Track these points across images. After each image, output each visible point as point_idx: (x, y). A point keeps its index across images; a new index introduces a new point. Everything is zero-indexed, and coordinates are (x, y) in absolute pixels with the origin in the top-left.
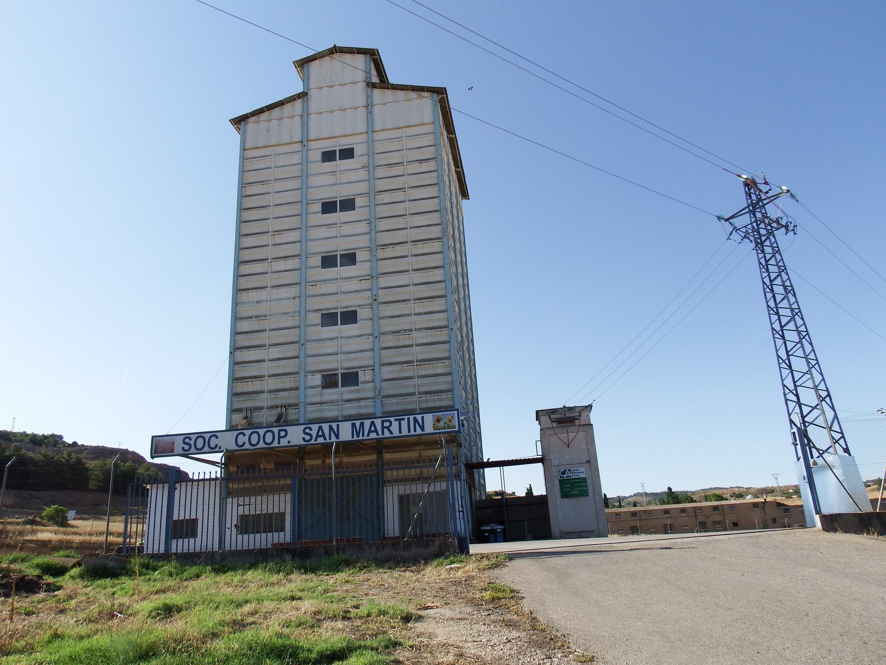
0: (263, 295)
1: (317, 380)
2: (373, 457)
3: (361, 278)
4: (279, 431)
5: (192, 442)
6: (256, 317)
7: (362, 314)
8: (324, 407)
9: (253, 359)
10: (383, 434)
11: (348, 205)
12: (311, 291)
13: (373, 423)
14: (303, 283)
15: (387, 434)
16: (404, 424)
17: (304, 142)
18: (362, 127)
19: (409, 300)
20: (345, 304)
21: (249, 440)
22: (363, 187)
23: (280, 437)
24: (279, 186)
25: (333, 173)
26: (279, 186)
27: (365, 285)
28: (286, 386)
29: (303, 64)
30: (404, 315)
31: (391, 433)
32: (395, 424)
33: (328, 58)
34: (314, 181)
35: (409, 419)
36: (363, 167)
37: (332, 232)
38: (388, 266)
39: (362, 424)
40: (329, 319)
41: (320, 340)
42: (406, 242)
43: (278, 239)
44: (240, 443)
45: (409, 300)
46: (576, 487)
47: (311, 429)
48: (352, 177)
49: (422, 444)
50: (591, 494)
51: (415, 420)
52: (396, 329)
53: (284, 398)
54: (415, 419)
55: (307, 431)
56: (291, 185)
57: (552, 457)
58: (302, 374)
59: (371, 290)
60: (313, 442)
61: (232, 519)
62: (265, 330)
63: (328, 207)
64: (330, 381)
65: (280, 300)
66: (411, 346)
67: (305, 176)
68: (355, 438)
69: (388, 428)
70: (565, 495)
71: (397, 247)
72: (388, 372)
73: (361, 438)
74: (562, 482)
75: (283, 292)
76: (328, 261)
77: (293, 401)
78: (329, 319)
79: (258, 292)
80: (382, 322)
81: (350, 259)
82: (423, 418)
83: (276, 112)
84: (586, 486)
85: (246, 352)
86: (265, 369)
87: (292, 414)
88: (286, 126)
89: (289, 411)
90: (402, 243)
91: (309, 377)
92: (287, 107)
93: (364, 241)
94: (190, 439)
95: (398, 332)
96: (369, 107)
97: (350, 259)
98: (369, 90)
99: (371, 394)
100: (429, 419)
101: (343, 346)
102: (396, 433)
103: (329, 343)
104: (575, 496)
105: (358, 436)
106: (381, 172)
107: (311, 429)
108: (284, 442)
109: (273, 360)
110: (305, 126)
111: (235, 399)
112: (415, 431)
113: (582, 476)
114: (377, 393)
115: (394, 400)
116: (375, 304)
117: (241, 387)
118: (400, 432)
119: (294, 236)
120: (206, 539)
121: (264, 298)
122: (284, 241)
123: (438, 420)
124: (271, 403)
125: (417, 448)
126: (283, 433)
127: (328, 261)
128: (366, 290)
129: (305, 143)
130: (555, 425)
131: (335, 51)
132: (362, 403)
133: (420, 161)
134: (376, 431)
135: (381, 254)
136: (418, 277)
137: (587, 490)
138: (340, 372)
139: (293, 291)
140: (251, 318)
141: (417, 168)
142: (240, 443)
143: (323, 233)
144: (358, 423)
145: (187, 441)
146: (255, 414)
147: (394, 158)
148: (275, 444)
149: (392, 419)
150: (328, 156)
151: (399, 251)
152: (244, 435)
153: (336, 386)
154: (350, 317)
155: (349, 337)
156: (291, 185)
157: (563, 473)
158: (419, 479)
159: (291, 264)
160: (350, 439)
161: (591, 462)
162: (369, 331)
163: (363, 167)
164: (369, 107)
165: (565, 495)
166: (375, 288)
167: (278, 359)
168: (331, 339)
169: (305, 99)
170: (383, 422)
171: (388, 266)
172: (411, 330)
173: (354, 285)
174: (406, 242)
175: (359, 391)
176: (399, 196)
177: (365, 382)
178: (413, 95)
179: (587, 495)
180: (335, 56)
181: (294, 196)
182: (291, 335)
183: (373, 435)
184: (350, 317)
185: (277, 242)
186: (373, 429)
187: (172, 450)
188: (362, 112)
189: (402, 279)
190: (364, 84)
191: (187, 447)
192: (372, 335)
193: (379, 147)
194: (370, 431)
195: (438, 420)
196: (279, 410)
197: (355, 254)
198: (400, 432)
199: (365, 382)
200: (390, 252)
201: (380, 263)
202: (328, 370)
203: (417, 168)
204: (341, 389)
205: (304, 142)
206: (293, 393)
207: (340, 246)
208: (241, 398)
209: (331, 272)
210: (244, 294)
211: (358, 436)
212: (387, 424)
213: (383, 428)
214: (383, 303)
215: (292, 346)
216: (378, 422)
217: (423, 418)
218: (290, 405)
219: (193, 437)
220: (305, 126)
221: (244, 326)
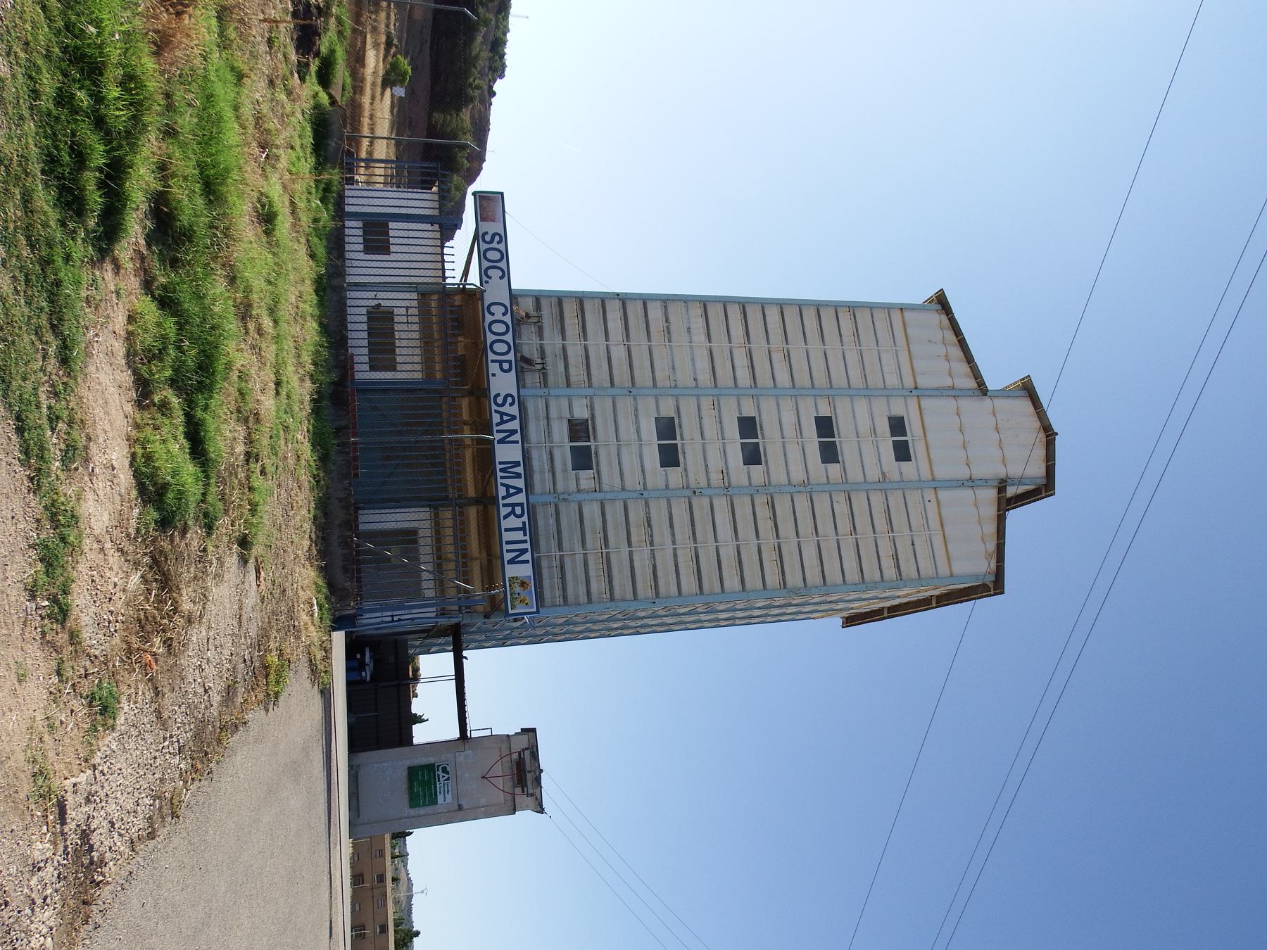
0: (699, 336)
1: (581, 412)
2: (471, 492)
3: (725, 472)
4: (510, 362)
5: (494, 245)
7: (675, 474)
8: (543, 423)
9: (610, 325)
10: (504, 505)
11: (830, 453)
12: (706, 403)
13: (520, 490)
15: (504, 511)
16: (519, 535)
17: (917, 392)
18: (942, 472)
19: (695, 541)
21: (496, 320)
22: (855, 474)
23: (501, 362)
24: (852, 358)
26: (852, 358)
27: (716, 478)
28: (572, 370)
29: (1027, 389)
30: (673, 535)
31: (505, 517)
33: (1038, 424)
34: (861, 406)
35: (525, 541)
36: (884, 474)
37: (790, 431)
38: (743, 511)
39: (518, 476)
40: (667, 428)
41: (636, 416)
42: (778, 536)
43: (778, 357)
44: (493, 309)
45: (695, 541)
46: (424, 790)
47: (511, 405)
48: (870, 459)
49: (490, 561)
50: (412, 812)
51: (524, 551)
52: (653, 522)
53: (555, 369)
54: (525, 551)
55: (509, 400)
56: (855, 374)
57: (469, 752)
58: (590, 392)
59: (709, 486)
60: (494, 407)
61: (387, 300)
62: (649, 340)
63: (825, 426)
64: (579, 430)
65: (693, 360)
66: (630, 545)
67: (868, 393)
68: (499, 467)
69: (513, 512)
70: (412, 772)
71: (770, 523)
72: (592, 511)
73: (499, 474)
74: (431, 768)
75: (703, 364)
76: (748, 426)
77: (551, 379)
78: (667, 428)
79: (703, 331)
80: (663, 503)
81: (753, 456)
82: (527, 562)
83: (956, 352)
84: (424, 805)
85: (619, 314)
86: (596, 341)
87: (532, 379)
88: (937, 366)
91: (585, 402)
92: (964, 368)
93: (778, 476)
95: (649, 526)
96: (971, 483)
97: (753, 456)
98: (996, 483)
99: (560, 486)
100: (525, 571)
101: (628, 448)
102: (506, 524)
103: (633, 430)
104: (411, 787)
105: (501, 470)
107: (511, 405)
108: (494, 368)
109: (608, 352)
110: (939, 392)
111: (554, 301)
112: (508, 551)
113: (440, 798)
115: (552, 521)
116: (688, 493)
117: (570, 310)
118: (507, 530)
119: (783, 378)
120: (362, 266)
121: (694, 338)
122: (775, 365)
123: (523, 584)
124: (548, 350)
125: (484, 555)
126: (506, 366)
127: (748, 426)
128: (708, 480)
130: (515, 756)
131: (1049, 435)
132: (548, 476)
133: (896, 557)
134: (509, 495)
135: (761, 500)
136: (728, 554)
137: (419, 806)
138: (592, 443)
139: (705, 377)
140: (667, 321)
141: (886, 551)
142: (493, 309)
143: (789, 418)
144: (520, 470)
145: (497, 238)
146: (533, 329)
148: (491, 356)
149: (525, 518)
150: (897, 425)
151: (765, 526)
152: (504, 314)
153: (572, 439)
154: (670, 457)
155: (641, 457)
156: (855, 374)
157: (445, 770)
158: (439, 557)
161: (459, 813)
162: (649, 486)
163: (884, 474)
164: (971, 483)
165: (412, 772)
166: (710, 492)
168: (638, 432)
170: (521, 505)
171: (743, 511)
172: (652, 544)
173: (715, 462)
174: (778, 536)
175: (565, 471)
176: (845, 526)
177: (577, 480)
178: (992, 546)
179: (411, 807)
180: (1042, 435)
181: (839, 379)
182: (643, 375)
183: (502, 491)
184: (670, 457)
186: (512, 491)
187: (483, 219)
188: (963, 473)
190: (1003, 475)
191: (488, 238)
192: (645, 488)
193: (914, 497)
194: (508, 487)
195: (523, 584)
196: (539, 361)
198: (507, 530)
199: (577, 480)
200: (763, 513)
201: (747, 500)
202: (594, 428)
203: (886, 551)
204: (568, 445)
205: (917, 392)
206: (562, 379)
207: (770, 442)
208: (555, 310)
209: (733, 430)
210: (700, 311)
211: (501, 470)
212: (518, 510)
213: (513, 505)
215: (627, 377)
216: (521, 498)
217: (527, 562)
218: (545, 376)
220: (939, 392)
221: (655, 313)
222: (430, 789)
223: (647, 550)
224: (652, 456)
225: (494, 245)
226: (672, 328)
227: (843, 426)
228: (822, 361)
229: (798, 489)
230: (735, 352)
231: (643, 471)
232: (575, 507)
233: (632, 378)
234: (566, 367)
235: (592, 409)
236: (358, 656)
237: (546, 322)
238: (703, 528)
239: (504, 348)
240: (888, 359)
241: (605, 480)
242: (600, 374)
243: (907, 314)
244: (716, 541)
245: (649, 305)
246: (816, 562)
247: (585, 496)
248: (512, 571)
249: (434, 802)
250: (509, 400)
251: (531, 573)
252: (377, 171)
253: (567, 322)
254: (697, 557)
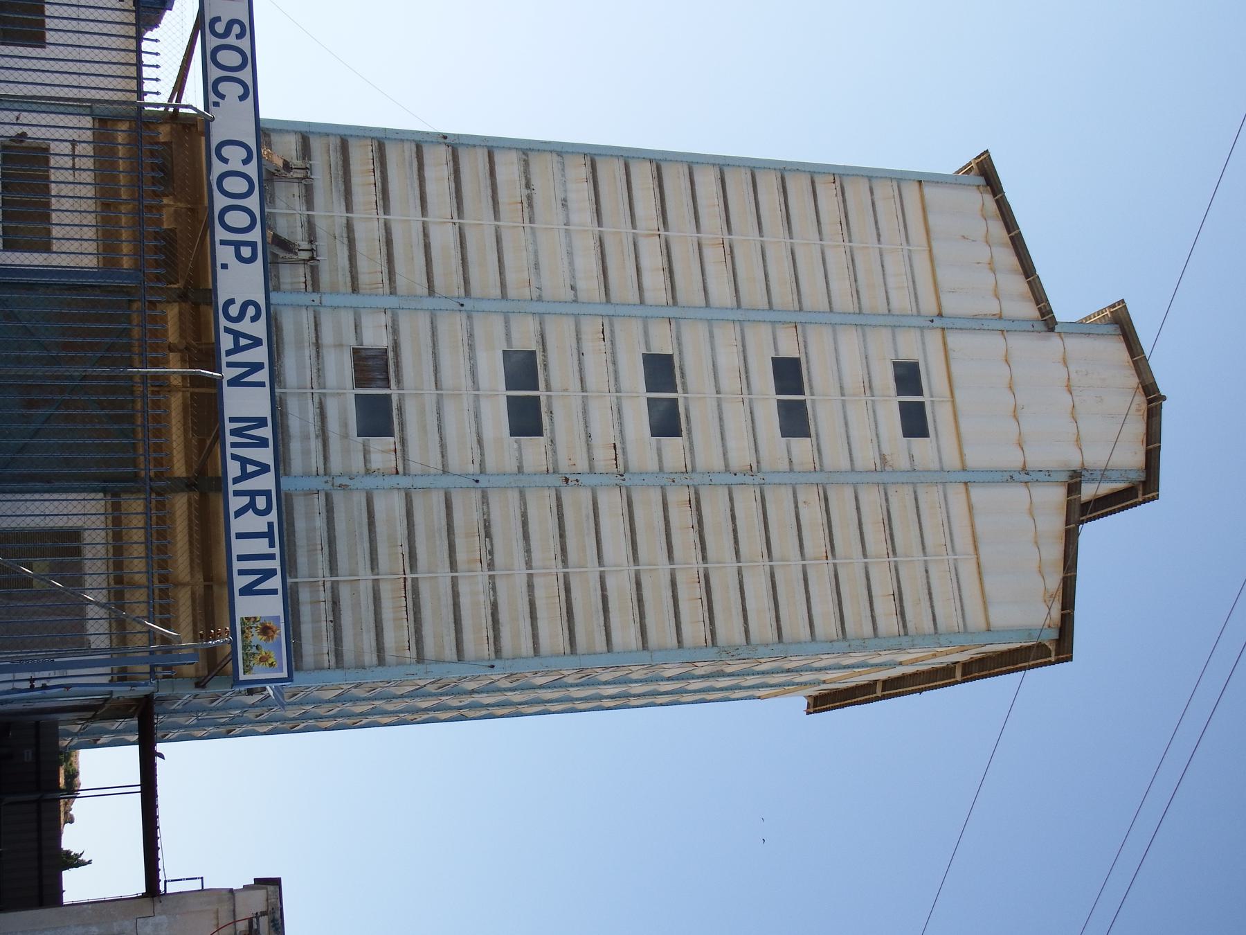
0: (582, 214)
1: (375, 337)
2: (179, 469)
4: (253, 245)
5: (231, 40)
6: (529, 198)
7: (534, 448)
8: (309, 352)
9: (430, 188)
10: (237, 493)
11: (795, 420)
12: (591, 328)
13: (264, 468)
14: (609, 310)
15: (236, 503)
16: (261, 546)
17: (940, 321)
18: (977, 457)
19: (565, 561)
20: (557, 407)
21: (231, 173)
22: (835, 457)
23: (237, 245)
24: (837, 260)
25: (870, 387)
26: (837, 260)
27: (603, 457)
28: (363, 265)
29: (1120, 322)
30: (528, 551)
31: (239, 513)
32: (256, 523)
33: (1134, 381)
34: (850, 342)
35: (272, 557)
36: (883, 458)
37: (730, 382)
39: (263, 443)
40: (523, 369)
41: (471, 347)
42: (704, 559)
43: (713, 255)
44: (227, 151)
45: (565, 561)
47: (254, 319)
48: (861, 431)
49: (208, 588)
51: (270, 573)
52: (496, 530)
55: (251, 311)
56: (841, 286)
57: (161, 919)
58: (392, 302)
59: (592, 470)
60: (223, 322)
63: (788, 374)
64: (372, 367)
65: (570, 254)
66: (453, 566)
67: (861, 320)
68: (229, 426)
69: (252, 505)
71: (693, 536)
72: (389, 508)
73: (230, 439)
75: (587, 263)
76: (660, 370)
77: (325, 278)
78: (523, 369)
79: (588, 205)
80: (514, 496)
81: (667, 422)
82: (274, 592)
83: (1008, 258)
85: (446, 171)
87: (293, 276)
88: (972, 276)
89: (301, 270)
90: (703, 549)
91: (383, 319)
92: (1021, 285)
93: (708, 457)
94: (240, 36)
95: (488, 535)
96: (1025, 476)
97: (667, 422)
98: (1064, 477)
99: (336, 464)
100: (269, 607)
101: (454, 401)
102: (237, 525)
103: (464, 370)
105: (234, 432)
106: (871, 499)
107: (254, 319)
108: (225, 254)
109: (426, 235)
110: (977, 323)
111: (334, 142)
112: (241, 572)
114: (338, 481)
115: (320, 523)
116: (557, 481)
117: (361, 159)
118: (240, 536)
119: (721, 291)
121: (574, 218)
123: (266, 630)
125: (199, 577)
126: (246, 252)
127: (660, 370)
128: (591, 460)
129: (937, 322)
130: (242, 926)
131: (1152, 398)
132: (315, 444)
133: (899, 597)
134: (245, 476)
135: (677, 497)
136: (620, 586)
138: (393, 392)
139: (590, 285)
140: (528, 186)
141: (883, 586)
142: (225, 151)
143: (729, 359)
144: (266, 432)
145: (236, 29)
146: (296, 189)
147: (905, 535)
148: (221, 234)
149: (273, 517)
150: (908, 377)
151: (684, 540)
152: (246, 162)
153: (359, 382)
154: (526, 419)
156: (841, 286)
158: (119, 580)
159: (655, 282)
160: (228, 413)
162: (490, 465)
163: (883, 458)
164: (1025, 476)
167: (427, 247)
169: (1040, 326)
170: (267, 493)
172: (491, 566)
173: (603, 431)
174: (704, 559)
175: (345, 436)
176: (815, 542)
177: (366, 452)
180: (1141, 399)
181: (814, 295)
182: (484, 277)
183: (234, 469)
184: (526, 419)
185: (706, 251)
186: (250, 468)
188: (1013, 459)
189: (616, 547)
190: (1076, 465)
191: (220, 27)
192: (483, 471)
193: (931, 497)
194: (244, 461)
195: (266, 630)
196: (305, 245)
197: (677, 433)
198: (240, 536)
199: (366, 452)
200: (681, 517)
201: (656, 496)
203: (883, 586)
204: (351, 393)
205: (940, 321)
206: (344, 279)
207: (696, 398)
208: (335, 158)
209: (634, 376)
210: (584, 172)
211: (234, 432)
212: (261, 502)
213: (253, 494)
214: (559, 499)
215: (458, 279)
216: (266, 482)
217: (274, 592)
218: (314, 272)
219: (244, 44)
220: (977, 323)
221: (508, 170)
223: (482, 576)
224: (496, 416)
225: (231, 40)
227: (818, 375)
228: (787, 263)
229: (740, 478)
232: (359, 499)
233: (466, 281)
235: (395, 331)
237: (320, 178)
239: (244, 220)
240: (896, 266)
241: (414, 453)
242: (410, 272)
243: (929, 191)
244: (601, 563)
245: (499, 158)
246: (767, 603)
248: (246, 607)
250: (251, 311)
253: (356, 180)
254: (568, 590)
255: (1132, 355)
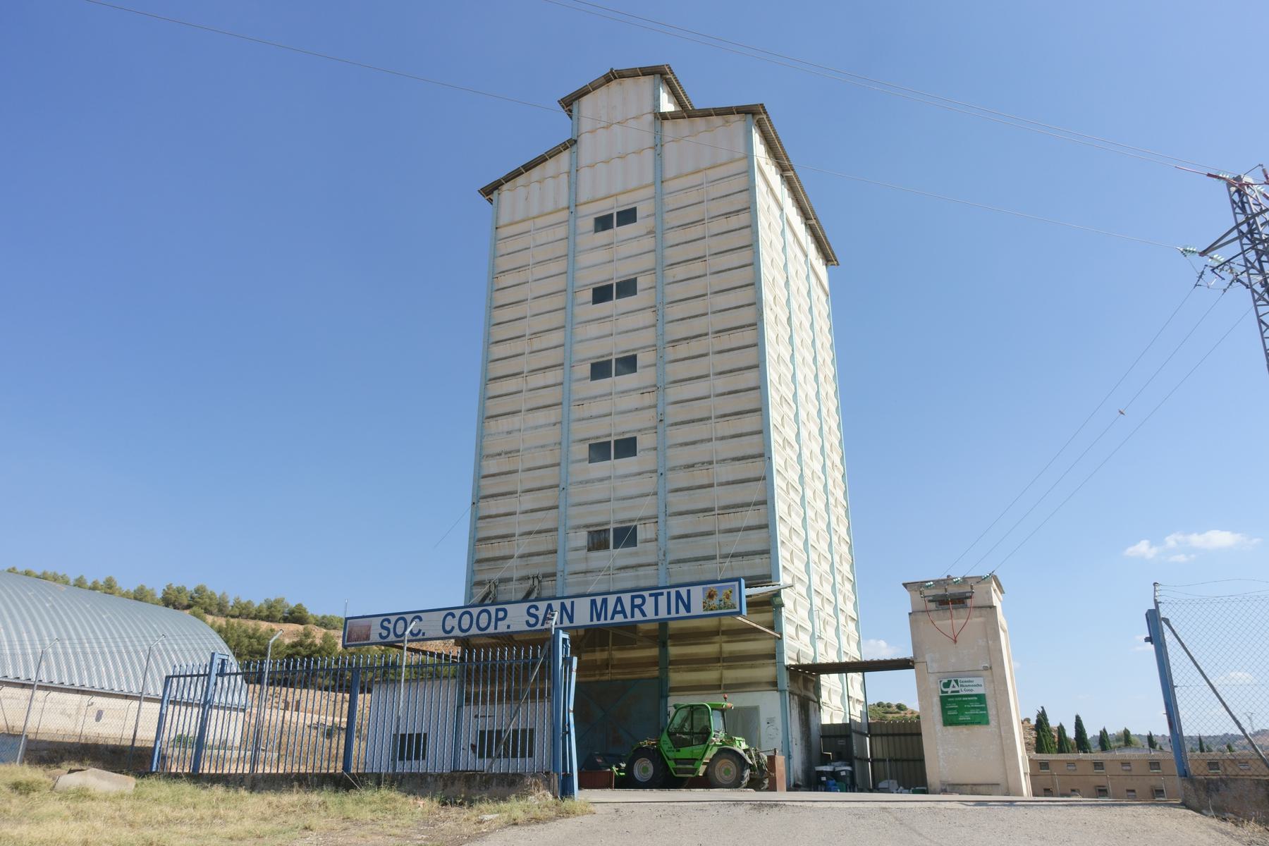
0: (515, 422)
1: (582, 538)
2: (654, 652)
3: (643, 391)
4: (498, 610)
5: (391, 626)
6: (506, 453)
7: (643, 442)
8: (589, 577)
9: (502, 510)
10: (633, 616)
11: (628, 288)
12: (577, 412)
13: (619, 600)
14: (566, 403)
15: (638, 616)
16: (662, 600)
17: (573, 207)
18: (649, 178)
19: (709, 418)
20: (620, 430)
21: (484, 623)
22: (648, 261)
23: (497, 620)
24: (540, 272)
25: (609, 245)
26: (540, 272)
27: (648, 399)
28: (543, 548)
29: (569, 103)
30: (702, 441)
31: (644, 615)
32: (650, 601)
33: (604, 88)
34: (585, 259)
35: (669, 593)
36: (649, 233)
37: (606, 328)
38: (682, 370)
39: (605, 601)
40: (600, 451)
41: (587, 482)
42: (706, 334)
43: (537, 344)
44: (448, 628)
45: (709, 418)
46: (968, 709)
47: (537, 609)
48: (633, 248)
49: (725, 633)
50: (993, 723)
51: (678, 595)
52: (690, 462)
53: (539, 566)
54: (678, 594)
55: (533, 611)
56: (554, 268)
57: (928, 658)
58: (561, 530)
59: (655, 406)
60: (539, 627)
61: (469, 736)
62: (516, 471)
63: (602, 294)
64: (598, 541)
65: (536, 428)
66: (711, 486)
67: (571, 255)
68: (595, 622)
69: (639, 607)
70: (948, 721)
71: (693, 343)
72: (678, 526)
73: (602, 621)
74: (944, 700)
75: (541, 417)
76: (600, 370)
77: (549, 570)
78: (600, 451)
79: (510, 419)
80: (670, 452)
81: (629, 364)
82: (689, 591)
83: (535, 173)
84: (985, 709)
85: (492, 502)
86: (517, 525)
87: (548, 587)
88: (544, 191)
89: (544, 583)
90: (700, 336)
91: (572, 535)
92: (550, 166)
93: (648, 337)
94: (389, 621)
95: (693, 466)
96: (658, 147)
97: (629, 364)
98: (658, 123)
99: (651, 559)
100: (698, 594)
101: (616, 490)
102: (650, 615)
103: (598, 485)
104: (966, 723)
105: (599, 619)
106: (673, 237)
107: (537, 609)
108: (502, 627)
109: (526, 512)
110: (573, 186)
111: (476, 567)
112: (677, 612)
113: (977, 691)
114: (662, 557)
115: (685, 567)
116: (661, 426)
117: (487, 552)
118: (656, 614)
119: (556, 338)
120: (437, 759)
121: (517, 427)
122: (544, 346)
123: (711, 596)
124: (523, 573)
125: (717, 639)
126: (501, 614)
127: (600, 370)
128: (650, 407)
129: (572, 209)
130: (932, 606)
131: (612, 77)
132: (641, 572)
133: (727, 215)
134: (623, 612)
135: (671, 353)
136: (723, 384)
137: (986, 716)
138: (612, 527)
139: (553, 415)
140: (500, 454)
141: (723, 225)
142: (448, 628)
143: (593, 330)
144: (599, 600)
145: (386, 624)
146: (502, 587)
147: (692, 214)
148: (491, 630)
149: (646, 594)
150: (603, 223)
151: (696, 347)
152: (454, 616)
153: (607, 547)
154: (627, 447)
155: (626, 476)
156: (554, 268)
157: (947, 685)
158: (719, 687)
159: (551, 377)
160: (589, 623)
161: (993, 668)
162: (653, 468)
163: (649, 233)
164: (658, 147)
165: (948, 721)
166: (660, 405)
167: (533, 511)
168: (601, 480)
169: (574, 148)
170: (633, 598)
171: (682, 370)
172: (711, 463)
173: (633, 401)
174: (706, 334)
175: (636, 554)
176: (697, 268)
177: (646, 541)
178: (717, 120)
179: (987, 723)
180: (614, 84)
181: (558, 284)
182: (548, 477)
183: (619, 618)
184: (627, 447)
185: (535, 348)
186: (619, 608)
187: (368, 638)
188: (649, 155)
189: (699, 388)
190: (650, 117)
191: (385, 633)
192: (656, 471)
193: (671, 202)
194: (615, 612)
195: (711, 596)
196: (531, 582)
197: (635, 357)
198: (656, 614)
199: (646, 541)
200: (683, 350)
201: (669, 367)
202: (597, 525)
203: (723, 225)
204: (613, 552)
205: (573, 207)
206: (550, 558)
207: (614, 349)
208: (485, 566)
209: (603, 384)
210: (492, 423)
211: (599, 619)
212: (638, 601)
213: (633, 606)
214: (672, 425)
215: (549, 492)
216: (626, 598)
217: (689, 591)
218: (545, 576)
219: (393, 619)
220: (573, 186)
221: (492, 466)
222: (968, 702)
223: (717, 468)
224: (626, 465)
225: (391, 626)
226: (507, 449)
227: (602, 276)
228: (542, 301)
229: (660, 318)
230: (531, 386)
231: (640, 474)
232: (672, 545)
233: (551, 487)
234: (538, 554)
235: (578, 527)
236: (824, 779)
237: (496, 576)
238: (697, 410)
239: (484, 616)
240: (543, 237)
241: (641, 513)
242: (547, 519)
243: (501, 223)
244: (709, 397)
245: (485, 472)
246: (732, 294)
247: (661, 533)
248: (697, 609)
249: (981, 698)
250: (533, 611)
251: (700, 588)
252: (177, 750)
253: (497, 554)
254: (725, 416)
255: (588, 92)
